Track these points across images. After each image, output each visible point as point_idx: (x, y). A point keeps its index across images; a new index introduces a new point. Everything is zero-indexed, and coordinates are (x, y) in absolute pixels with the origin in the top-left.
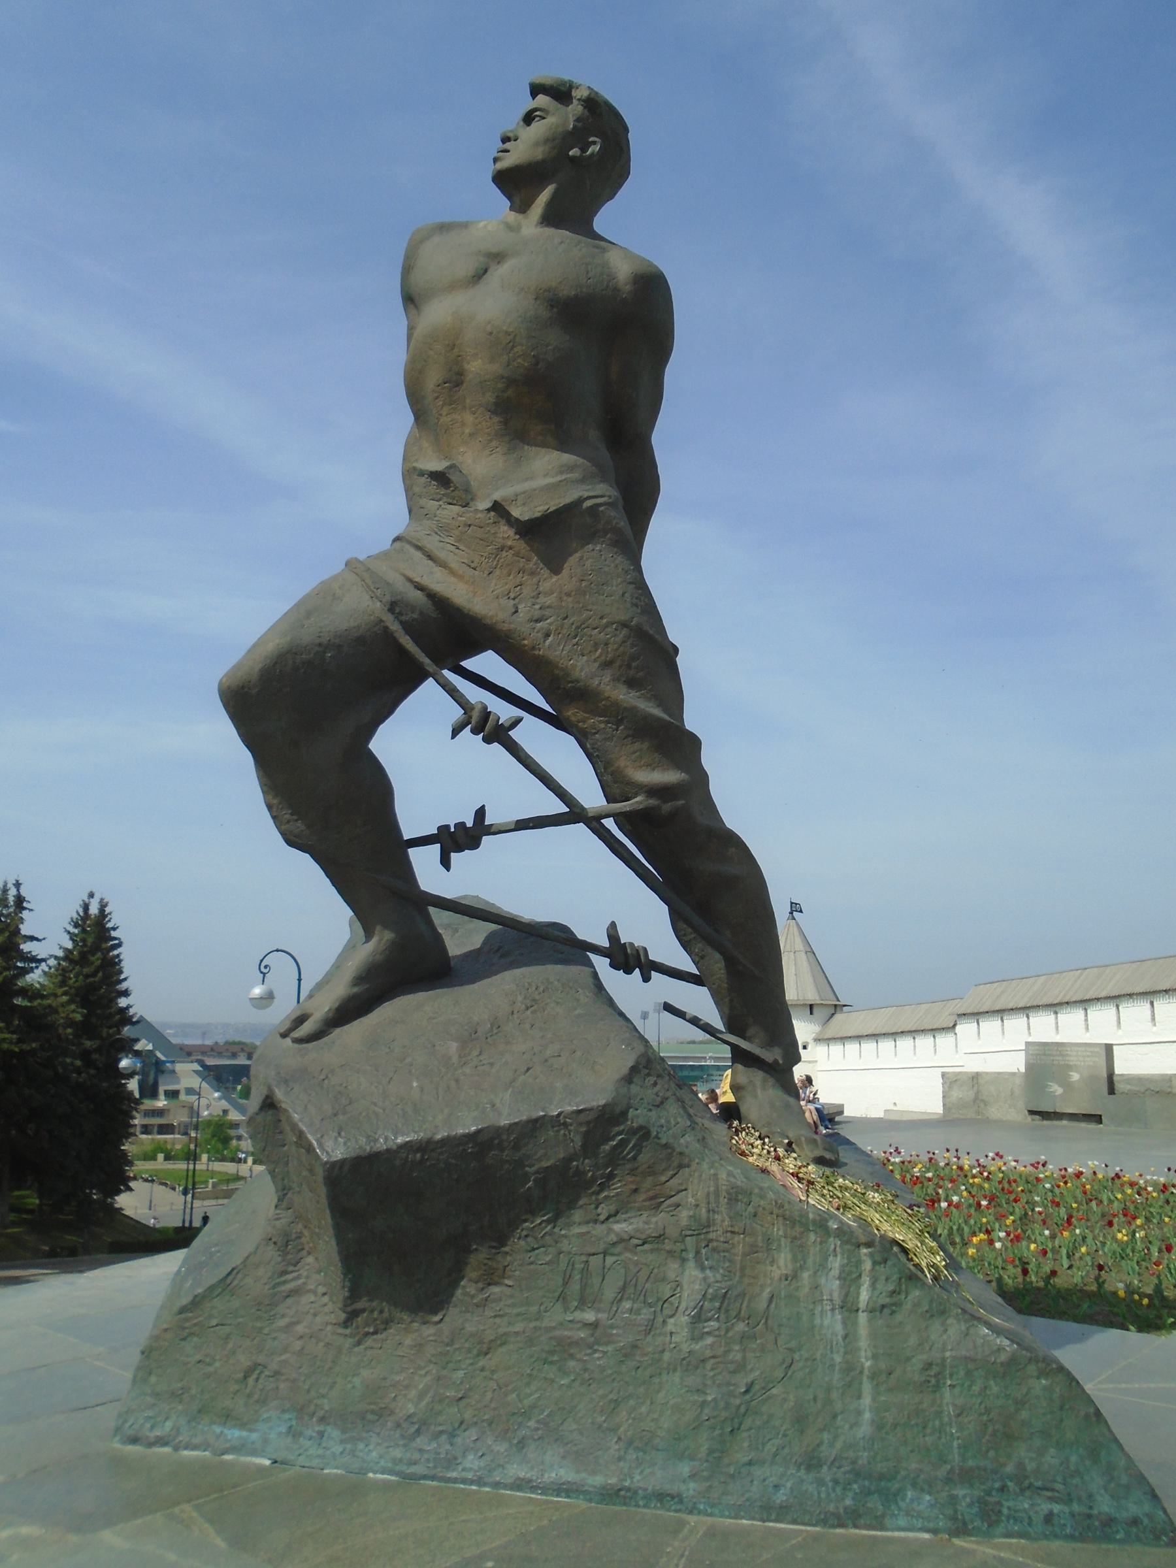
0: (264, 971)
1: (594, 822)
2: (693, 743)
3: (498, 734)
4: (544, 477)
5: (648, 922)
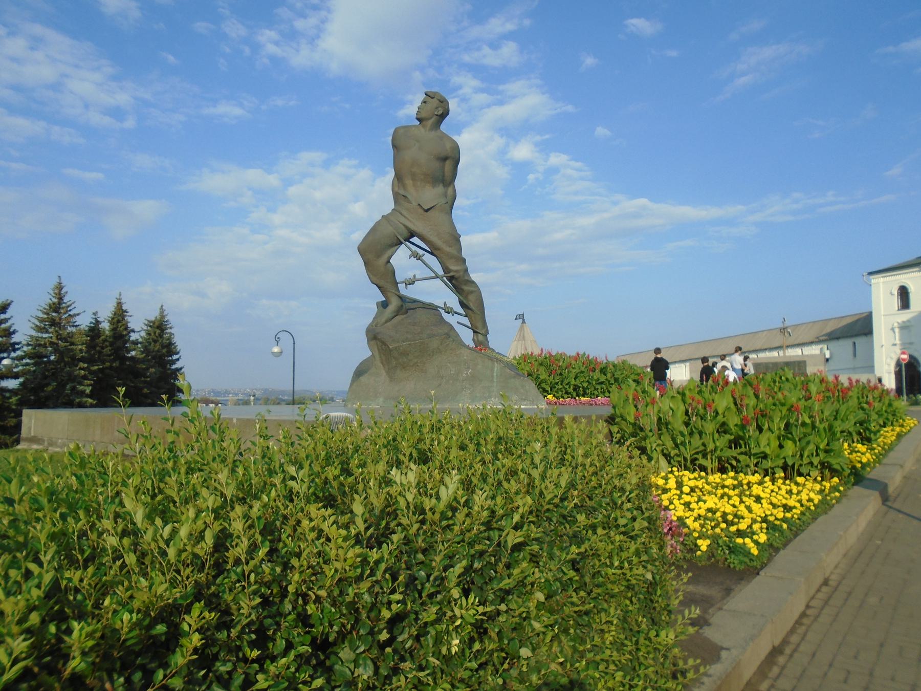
0: (277, 340)
1: (441, 278)
2: (464, 260)
3: (419, 258)
4: (430, 195)
5: (453, 300)
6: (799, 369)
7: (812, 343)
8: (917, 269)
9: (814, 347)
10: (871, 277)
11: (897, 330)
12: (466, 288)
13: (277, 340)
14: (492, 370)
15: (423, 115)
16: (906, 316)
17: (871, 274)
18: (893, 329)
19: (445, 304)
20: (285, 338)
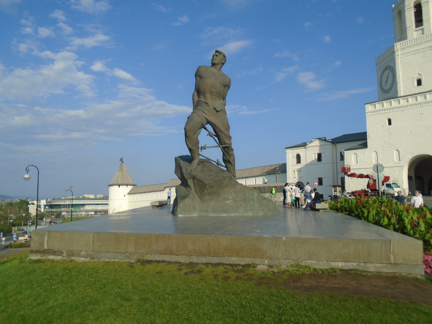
11: (296, 172)
12: (231, 153)
13: (27, 171)
14: (253, 196)
15: (215, 62)
16: (299, 166)
17: (286, 148)
18: (294, 171)
19: (217, 160)
20: (33, 171)
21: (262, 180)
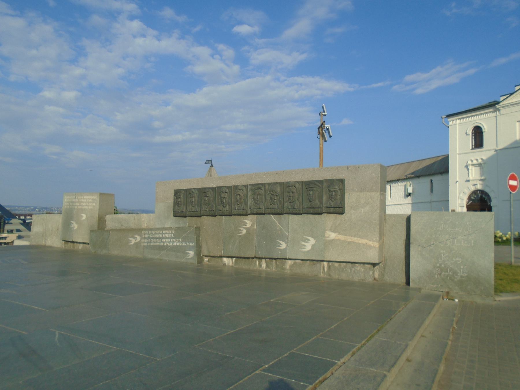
6: (330, 198)
7: (398, 180)
8: (491, 110)
9: (399, 184)
10: (449, 119)
17: (449, 116)
18: (467, 167)
21: (403, 188)
